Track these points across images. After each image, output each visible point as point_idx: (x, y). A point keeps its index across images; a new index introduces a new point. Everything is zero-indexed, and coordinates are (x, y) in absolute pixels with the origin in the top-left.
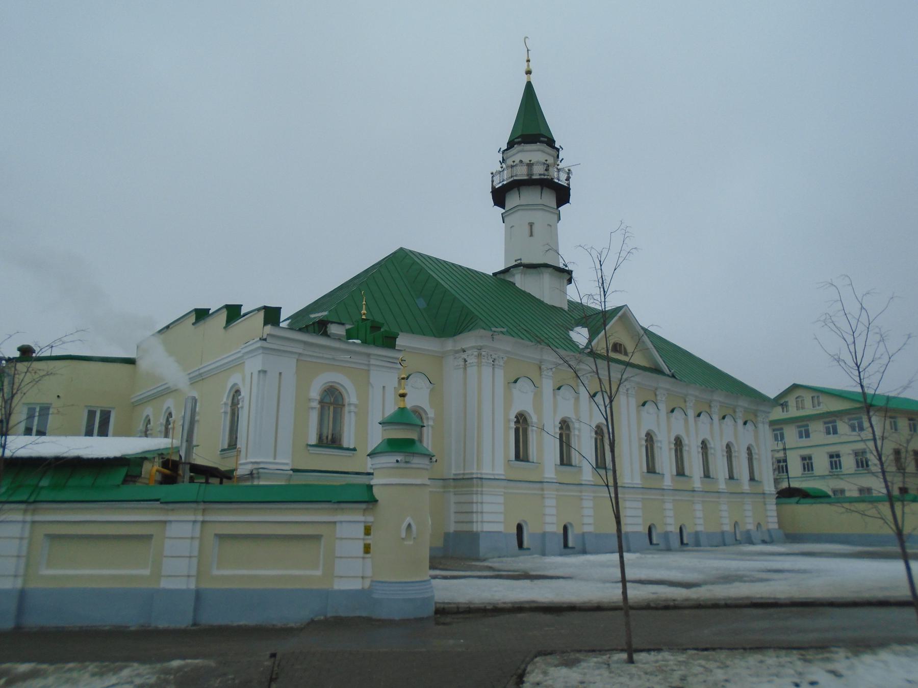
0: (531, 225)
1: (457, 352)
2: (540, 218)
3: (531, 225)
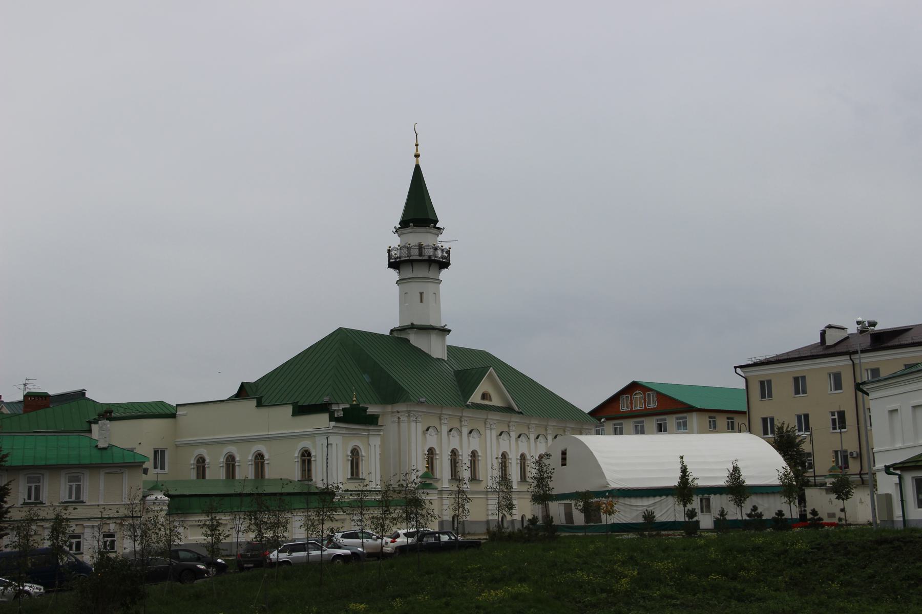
0: (421, 294)
1: (393, 412)
2: (428, 288)
3: (421, 294)
